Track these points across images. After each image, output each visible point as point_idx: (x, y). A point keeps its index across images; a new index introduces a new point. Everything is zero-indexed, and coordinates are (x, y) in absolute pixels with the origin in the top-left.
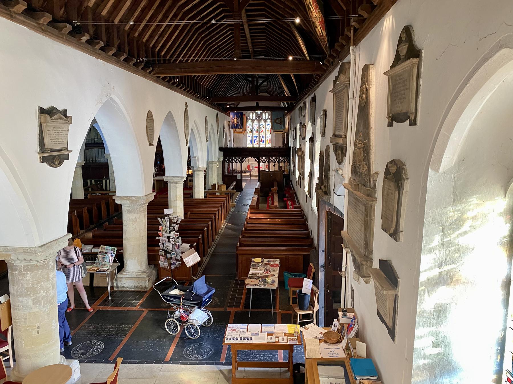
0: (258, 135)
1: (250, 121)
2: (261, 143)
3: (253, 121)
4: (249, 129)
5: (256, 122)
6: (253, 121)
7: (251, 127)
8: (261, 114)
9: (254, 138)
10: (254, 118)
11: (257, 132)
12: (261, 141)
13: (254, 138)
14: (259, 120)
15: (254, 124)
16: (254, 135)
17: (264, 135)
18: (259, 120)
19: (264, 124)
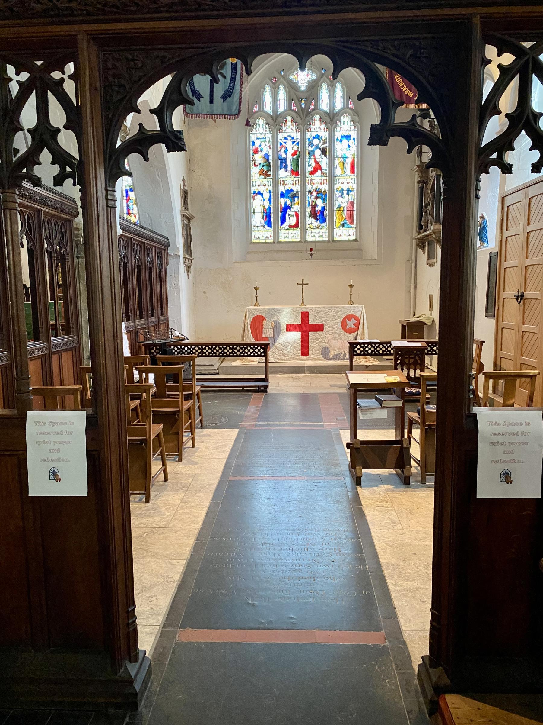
0: (296, 188)
1: (261, 122)
3: (275, 122)
4: (259, 158)
5: (289, 129)
6: (275, 122)
7: (266, 149)
8: (314, 86)
9: (282, 202)
10: (282, 107)
11: (295, 173)
12: (313, 214)
13: (282, 202)
14: (303, 118)
15: (281, 136)
16: (282, 189)
17: (325, 187)
18: (303, 118)
19: (324, 134)
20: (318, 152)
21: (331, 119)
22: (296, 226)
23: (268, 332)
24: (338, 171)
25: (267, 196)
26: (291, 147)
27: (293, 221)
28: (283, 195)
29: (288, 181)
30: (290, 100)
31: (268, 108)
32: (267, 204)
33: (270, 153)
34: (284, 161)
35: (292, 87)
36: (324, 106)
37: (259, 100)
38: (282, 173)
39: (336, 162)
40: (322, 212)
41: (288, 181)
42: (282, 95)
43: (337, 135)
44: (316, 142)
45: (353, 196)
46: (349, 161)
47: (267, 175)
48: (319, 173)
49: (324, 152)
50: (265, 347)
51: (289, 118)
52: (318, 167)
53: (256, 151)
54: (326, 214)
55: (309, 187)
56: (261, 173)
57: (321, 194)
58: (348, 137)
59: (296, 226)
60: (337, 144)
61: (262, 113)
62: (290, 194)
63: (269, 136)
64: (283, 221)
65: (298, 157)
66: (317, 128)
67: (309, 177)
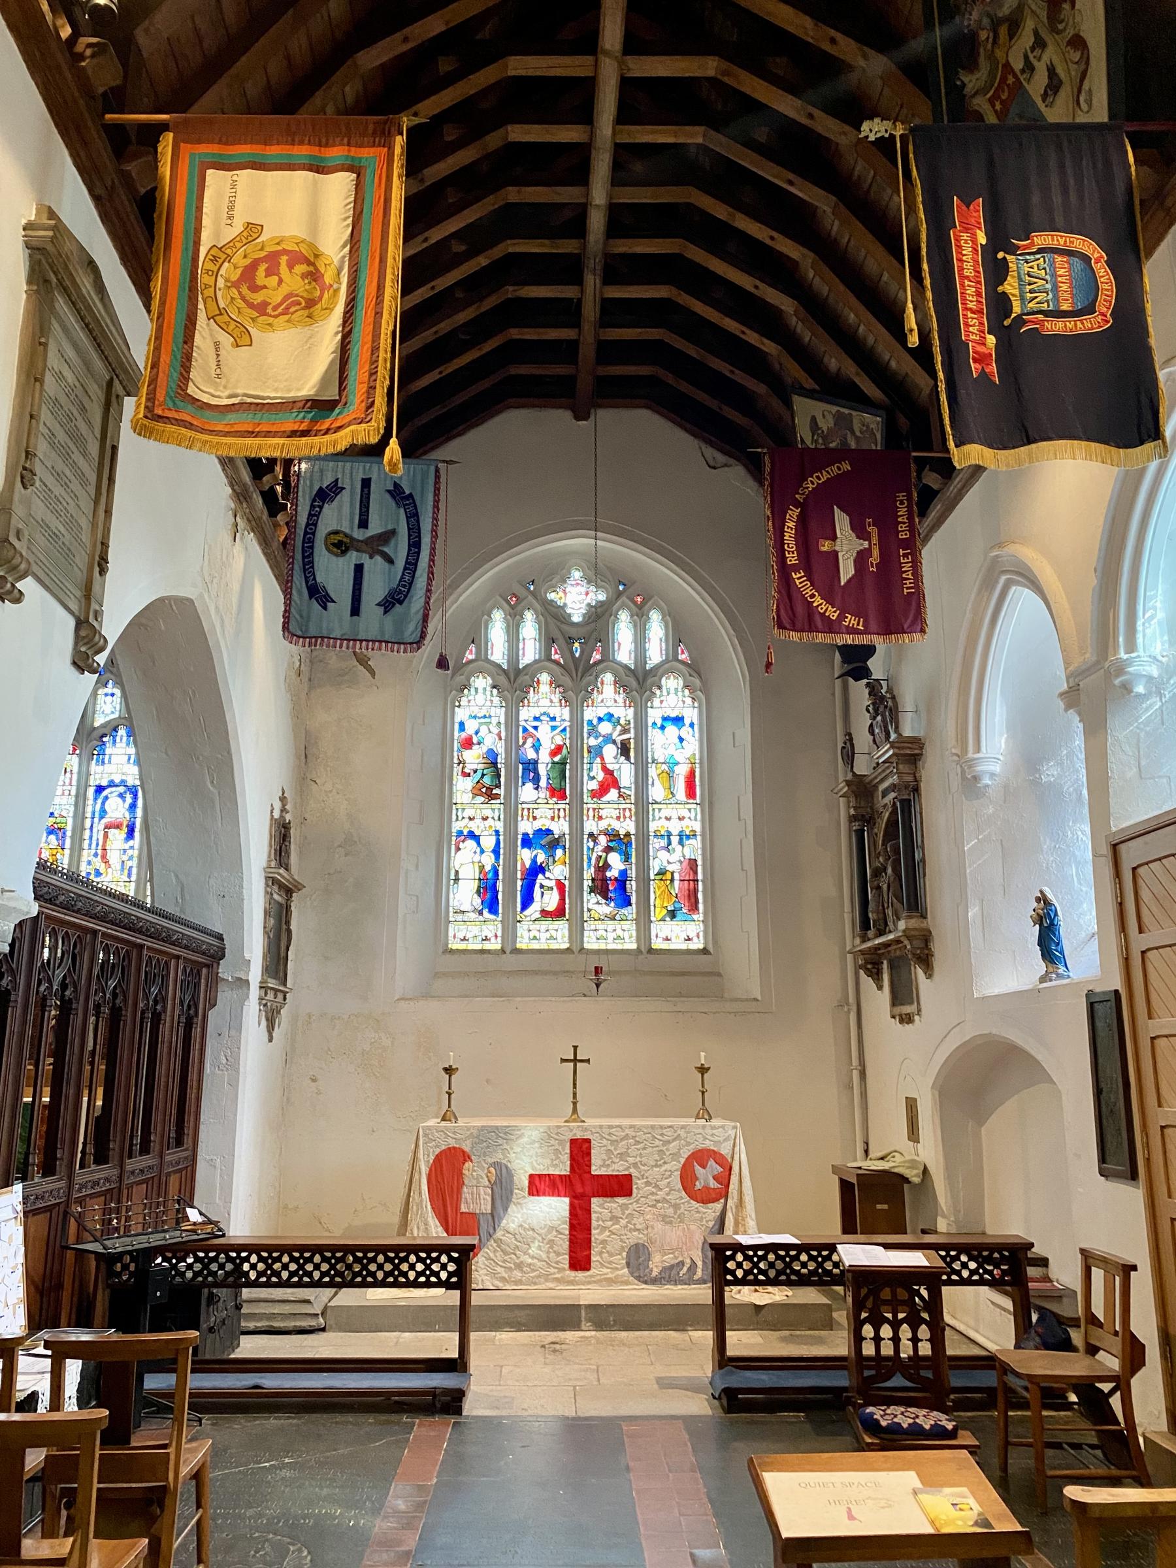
0: (560, 827)
1: (481, 682)
2: (594, 904)
3: (514, 683)
4: (473, 758)
5: (545, 699)
6: (514, 683)
7: (491, 740)
10: (530, 653)
11: (558, 793)
12: (601, 887)
14: (577, 678)
15: (525, 714)
16: (526, 827)
17: (627, 826)
18: (577, 678)
19: (626, 714)
20: (610, 751)
21: (640, 682)
22: (559, 913)
23: (475, 1197)
24: (657, 792)
25: (488, 842)
26: (548, 738)
27: (551, 901)
28: (527, 842)
29: (540, 811)
30: (548, 640)
31: (498, 653)
32: (488, 860)
33: (500, 749)
34: (531, 767)
35: (553, 616)
36: (624, 654)
37: (476, 636)
38: (527, 792)
39: (653, 772)
40: (622, 881)
41: (540, 811)
42: (530, 629)
43: (654, 715)
44: (605, 728)
45: (694, 849)
46: (682, 771)
47: (490, 796)
48: (613, 794)
49: (624, 750)
50: (465, 1253)
51: (545, 678)
52: (610, 781)
53: (468, 744)
54: (632, 886)
55: (590, 826)
56: (476, 792)
57: (618, 841)
58: (678, 720)
59: (559, 913)
60: (654, 735)
61: (484, 664)
62: (546, 840)
63: (499, 714)
64: (527, 901)
65: (565, 762)
66: (608, 699)
67: (590, 804)
